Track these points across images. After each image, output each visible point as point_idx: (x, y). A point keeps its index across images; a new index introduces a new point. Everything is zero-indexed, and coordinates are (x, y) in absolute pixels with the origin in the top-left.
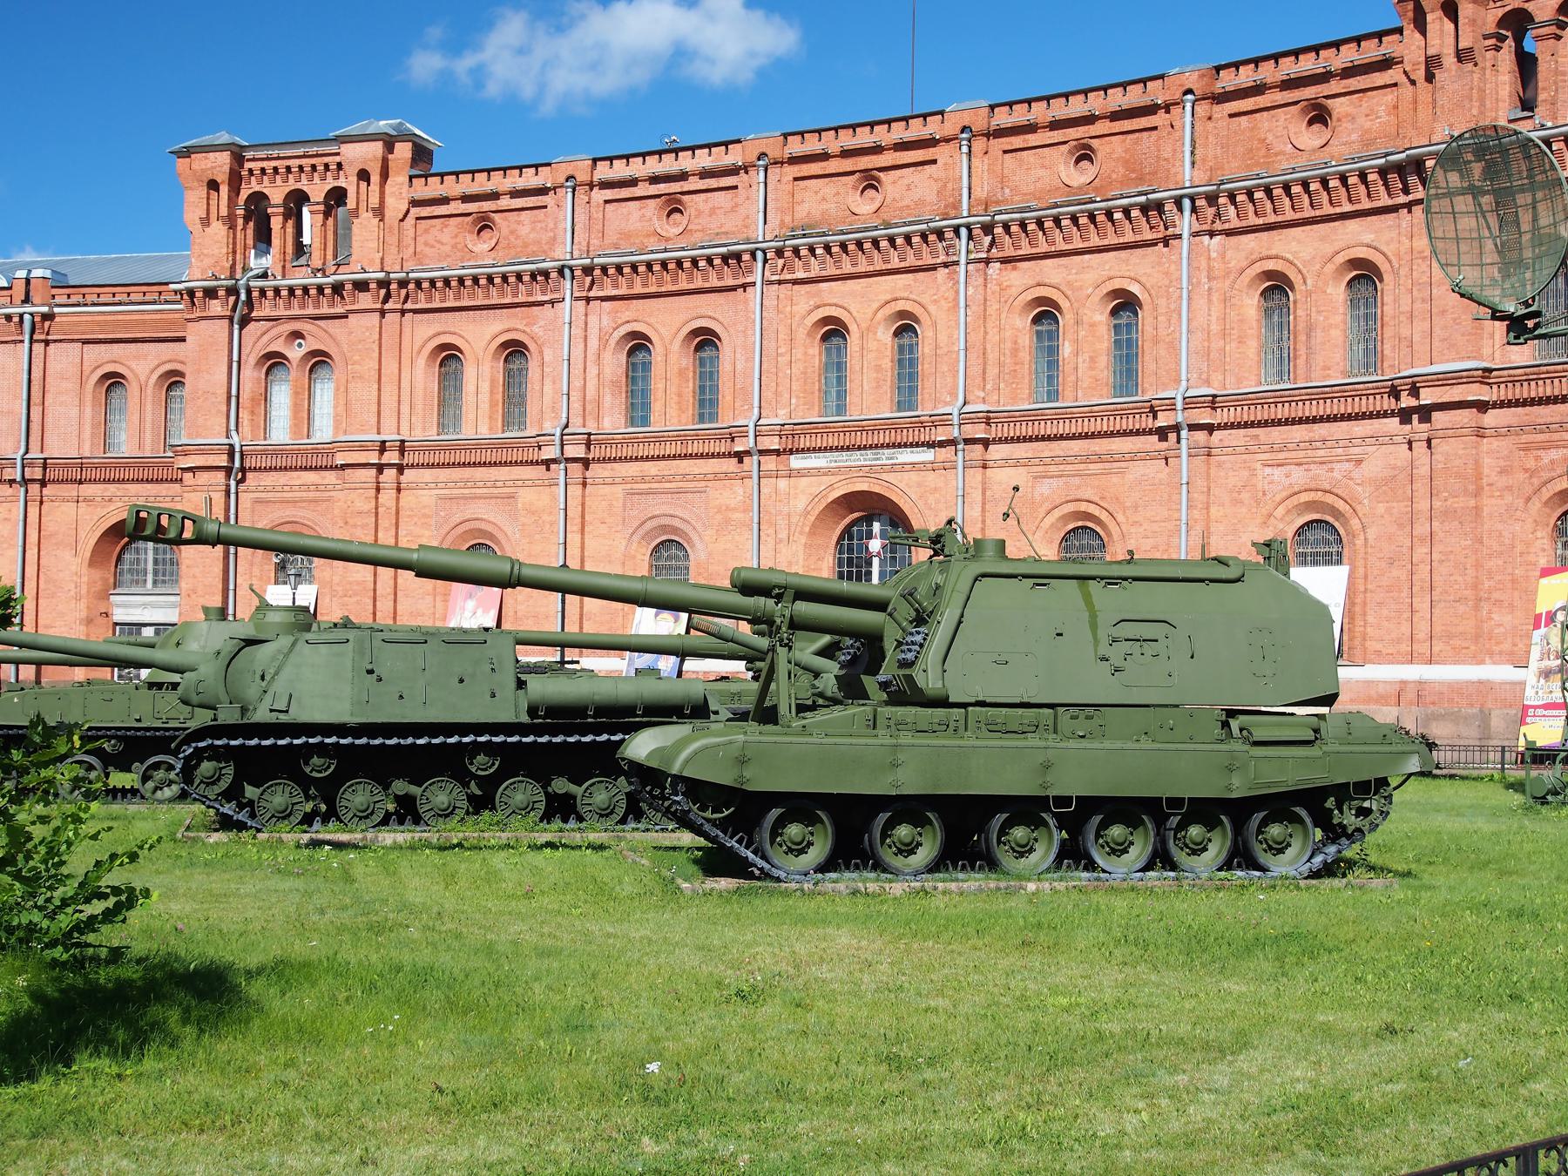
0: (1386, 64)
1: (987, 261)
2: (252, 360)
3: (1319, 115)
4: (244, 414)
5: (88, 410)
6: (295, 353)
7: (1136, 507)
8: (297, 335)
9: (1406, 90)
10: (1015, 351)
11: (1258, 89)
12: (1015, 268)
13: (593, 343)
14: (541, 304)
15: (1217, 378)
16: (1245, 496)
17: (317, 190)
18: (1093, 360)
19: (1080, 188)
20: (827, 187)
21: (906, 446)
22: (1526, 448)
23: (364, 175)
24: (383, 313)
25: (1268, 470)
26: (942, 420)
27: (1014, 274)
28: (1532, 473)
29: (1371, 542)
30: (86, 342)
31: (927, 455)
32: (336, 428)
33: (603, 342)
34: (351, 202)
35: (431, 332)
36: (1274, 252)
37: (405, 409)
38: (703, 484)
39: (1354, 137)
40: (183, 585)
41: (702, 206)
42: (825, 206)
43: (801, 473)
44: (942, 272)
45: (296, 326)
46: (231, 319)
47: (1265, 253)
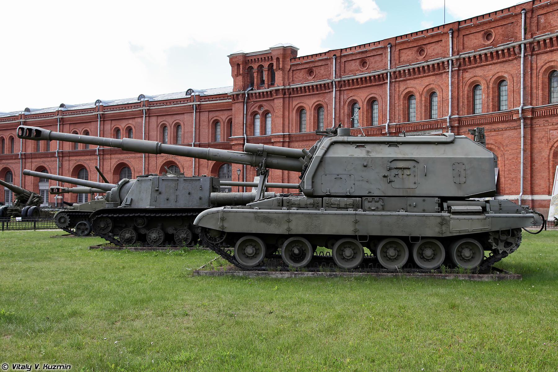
1: (459, 70)
2: (249, 114)
4: (248, 129)
5: (210, 130)
6: (261, 112)
7: (507, 145)
8: (260, 107)
10: (468, 98)
13: (342, 103)
14: (327, 93)
15: (534, 102)
16: (543, 140)
17: (266, 65)
18: (493, 99)
19: (488, 46)
20: (409, 52)
23: (278, 59)
24: (284, 98)
25: (551, 131)
26: (445, 120)
27: (467, 74)
30: (209, 111)
32: (272, 132)
33: (344, 104)
34: (275, 67)
35: (297, 103)
37: (291, 126)
40: (232, 177)
41: (372, 61)
42: (408, 57)
45: (261, 103)
46: (244, 102)
47: (550, 60)
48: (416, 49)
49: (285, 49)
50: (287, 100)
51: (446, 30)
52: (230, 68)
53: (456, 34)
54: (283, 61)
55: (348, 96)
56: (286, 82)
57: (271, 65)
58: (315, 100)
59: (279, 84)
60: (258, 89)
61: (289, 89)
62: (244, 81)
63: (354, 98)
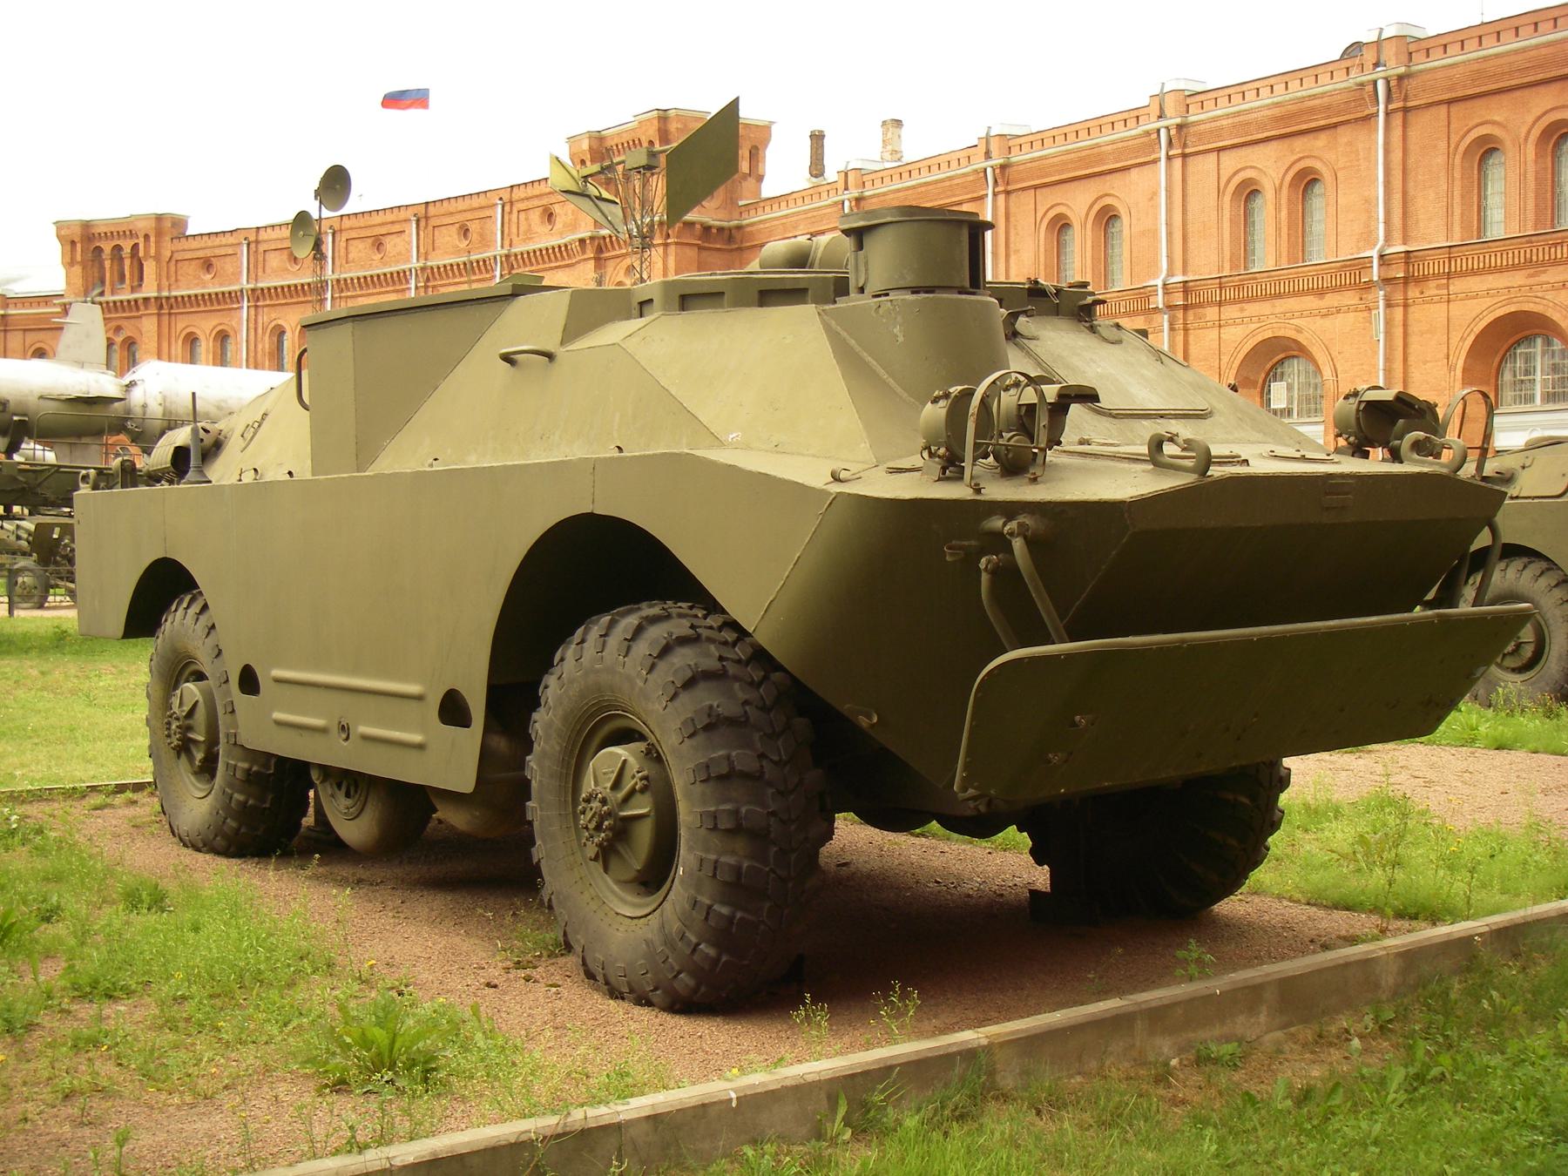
20: (360, 245)
23: (147, 237)
24: (159, 315)
34: (141, 254)
48: (370, 241)
49: (159, 218)
50: (166, 318)
51: (403, 215)
52: (55, 250)
53: (423, 223)
54: (157, 243)
55: (268, 317)
56: (165, 283)
57: (135, 246)
58: (214, 323)
59: (149, 290)
60: (113, 293)
61: (168, 298)
62: (85, 277)
63: (280, 322)
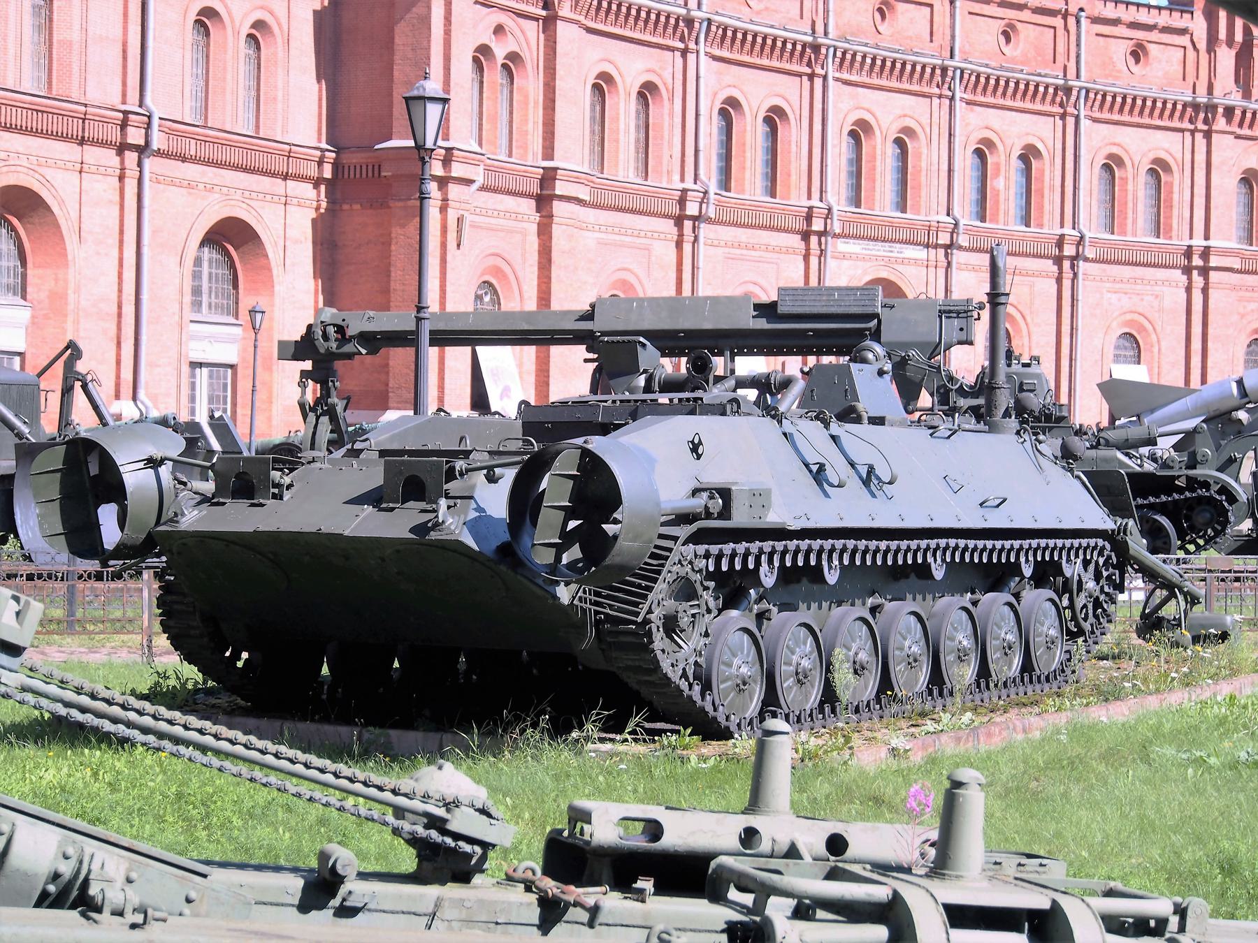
0: (1183, 32)
3: (1138, 53)
6: (500, 53)
9: (1191, 54)
11: (1115, 22)
12: (972, 110)
21: (912, 243)
22: (1241, 300)
25: (1109, 295)
28: (1243, 316)
29: (1163, 350)
31: (920, 253)
36: (1117, 141)
38: (776, 255)
39: (1160, 74)
43: (844, 256)
44: (936, 101)
